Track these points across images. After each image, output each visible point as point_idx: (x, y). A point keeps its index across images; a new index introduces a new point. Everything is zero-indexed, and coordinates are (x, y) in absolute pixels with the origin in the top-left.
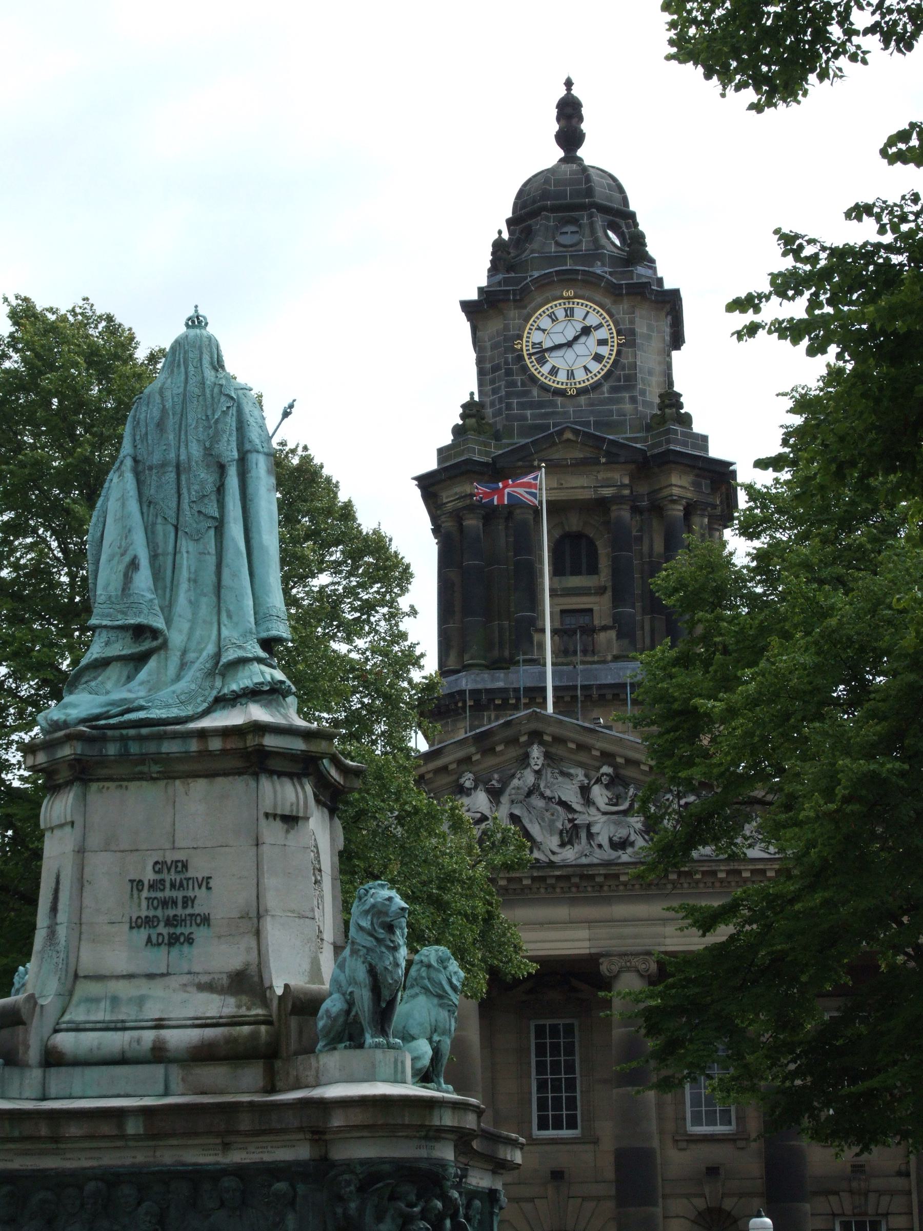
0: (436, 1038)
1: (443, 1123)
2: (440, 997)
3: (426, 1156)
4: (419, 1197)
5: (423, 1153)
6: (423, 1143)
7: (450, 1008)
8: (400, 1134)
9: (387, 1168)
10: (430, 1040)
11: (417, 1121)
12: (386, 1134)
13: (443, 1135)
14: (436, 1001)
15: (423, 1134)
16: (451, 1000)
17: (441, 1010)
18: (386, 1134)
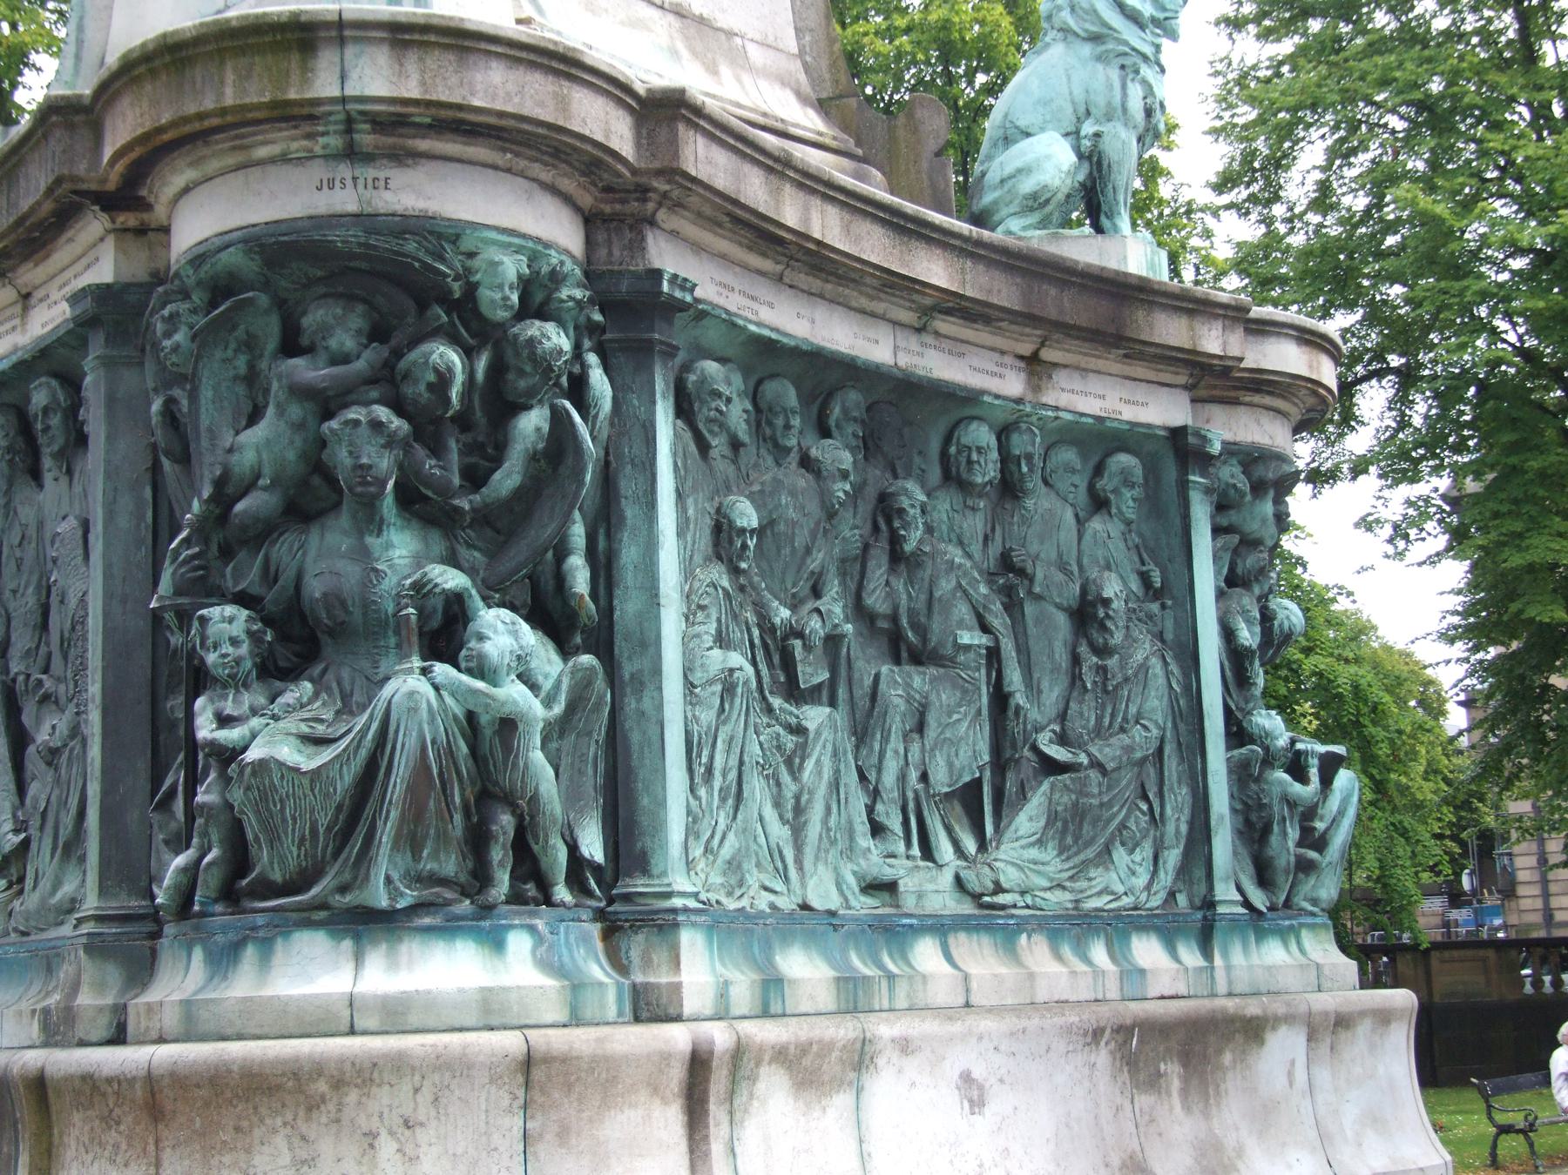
0: (1088, 128)
1: (351, 91)
2: (1095, 38)
3: (352, 207)
4: (377, 334)
5: (345, 201)
6: (344, 170)
7: (1128, 61)
8: (262, 152)
9: (232, 258)
10: (1074, 135)
11: (258, 93)
12: (231, 160)
13: (423, 145)
14: (1087, 50)
15: (335, 142)
16: (1126, 43)
17: (1100, 67)
18: (231, 160)
